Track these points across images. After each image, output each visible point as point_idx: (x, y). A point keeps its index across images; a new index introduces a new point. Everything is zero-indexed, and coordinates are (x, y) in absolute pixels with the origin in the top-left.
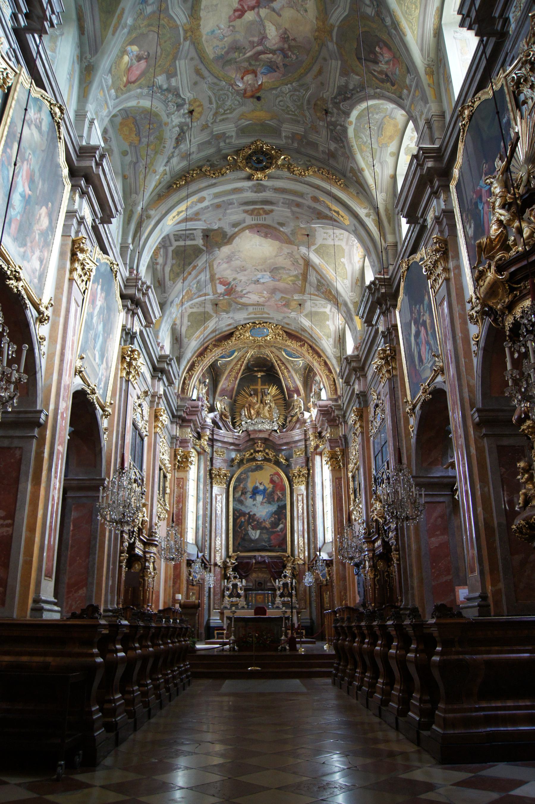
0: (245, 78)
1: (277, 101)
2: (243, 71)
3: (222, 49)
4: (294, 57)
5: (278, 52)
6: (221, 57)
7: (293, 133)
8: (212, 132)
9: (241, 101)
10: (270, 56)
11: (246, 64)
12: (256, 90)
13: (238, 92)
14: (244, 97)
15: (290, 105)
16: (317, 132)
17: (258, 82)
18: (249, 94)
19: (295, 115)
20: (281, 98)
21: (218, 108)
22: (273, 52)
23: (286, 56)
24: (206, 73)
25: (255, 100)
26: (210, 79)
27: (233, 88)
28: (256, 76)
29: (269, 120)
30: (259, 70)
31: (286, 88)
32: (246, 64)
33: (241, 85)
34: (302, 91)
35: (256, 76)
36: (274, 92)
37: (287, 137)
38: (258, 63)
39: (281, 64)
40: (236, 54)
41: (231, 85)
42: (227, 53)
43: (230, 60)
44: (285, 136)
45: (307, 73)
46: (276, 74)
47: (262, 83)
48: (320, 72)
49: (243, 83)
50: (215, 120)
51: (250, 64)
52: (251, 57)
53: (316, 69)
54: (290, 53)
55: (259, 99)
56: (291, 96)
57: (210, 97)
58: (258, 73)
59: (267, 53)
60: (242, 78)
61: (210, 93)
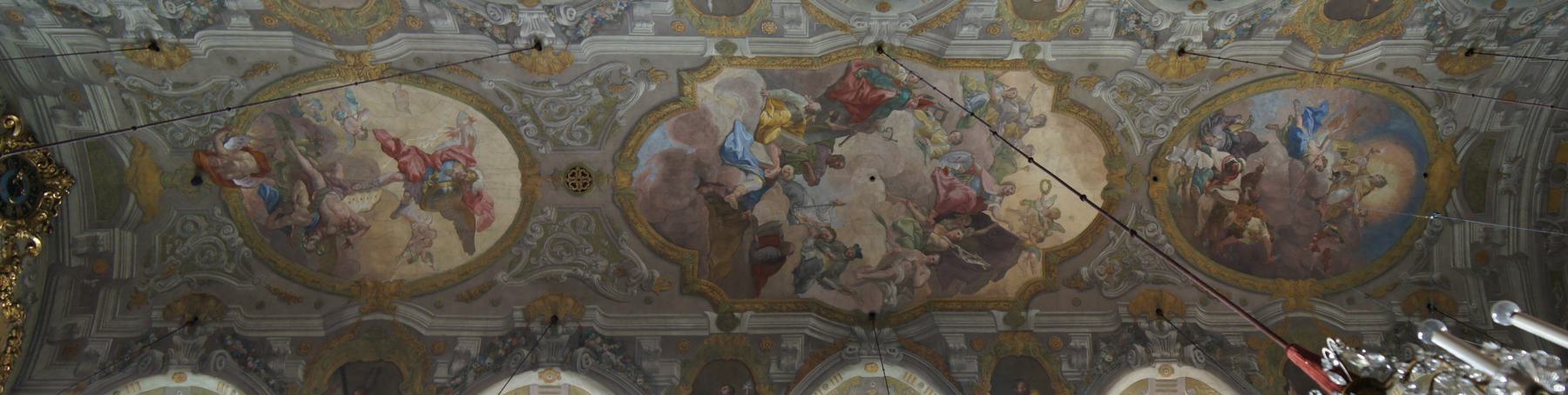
0: (246, 155)
1: (197, 218)
2: (265, 151)
3: (316, 115)
4: (311, 245)
5: (316, 216)
6: (296, 113)
7: (108, 257)
8: (90, 83)
9: (186, 145)
10: (306, 202)
11: (281, 155)
12: (219, 176)
13: (212, 139)
14: (196, 153)
15: (188, 243)
16: (128, 308)
17: (238, 178)
18: (206, 161)
19: (164, 256)
20: (202, 223)
21: (163, 98)
22: (315, 206)
23: (310, 230)
24: (257, 82)
25: (192, 174)
26: (241, 89)
27: (219, 131)
28: (253, 175)
29: (137, 201)
30: (270, 184)
31: (231, 233)
32: (281, 155)
33: (228, 146)
34: (233, 266)
35: (253, 175)
36: (218, 211)
37: (94, 241)
38: (285, 178)
39: (289, 223)
40: (304, 140)
41: (227, 127)
42: (306, 124)
43: (289, 129)
44: (96, 238)
45: (279, 274)
46: (263, 212)
47: (240, 187)
48: (287, 299)
49: (235, 151)
50: (127, 91)
51: (281, 165)
52: (300, 166)
53: (293, 289)
54: (317, 237)
55: (197, 181)
56: (214, 244)
57: (193, 85)
58: (261, 180)
59: (310, 195)
60: (246, 149)
61: (204, 86)
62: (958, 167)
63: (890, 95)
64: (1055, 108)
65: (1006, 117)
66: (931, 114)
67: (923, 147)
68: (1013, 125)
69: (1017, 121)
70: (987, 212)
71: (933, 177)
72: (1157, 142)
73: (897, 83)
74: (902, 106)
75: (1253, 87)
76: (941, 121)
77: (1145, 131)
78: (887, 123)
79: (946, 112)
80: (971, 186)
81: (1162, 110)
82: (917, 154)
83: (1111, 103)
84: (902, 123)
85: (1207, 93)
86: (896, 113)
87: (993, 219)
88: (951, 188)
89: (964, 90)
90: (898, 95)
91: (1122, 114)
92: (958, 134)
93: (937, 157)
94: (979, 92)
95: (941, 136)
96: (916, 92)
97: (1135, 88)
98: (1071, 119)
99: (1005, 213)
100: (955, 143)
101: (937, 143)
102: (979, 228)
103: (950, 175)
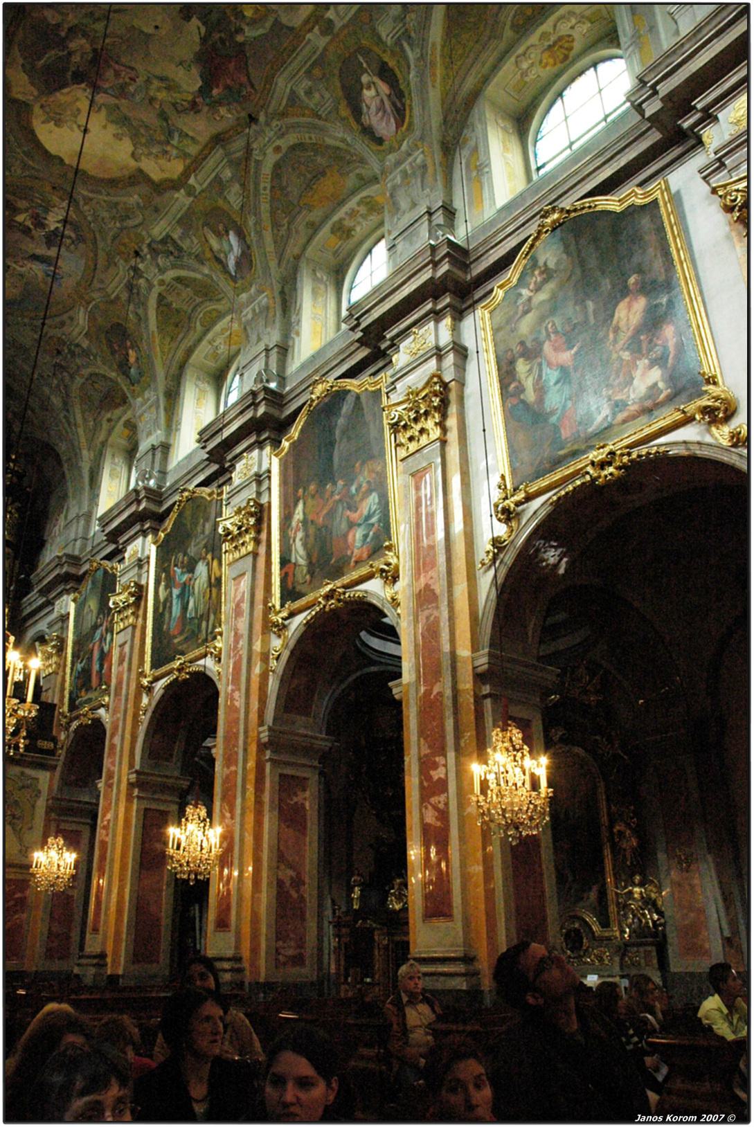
62: (132, 89)
63: (215, 92)
64: (140, 171)
65: (151, 141)
66: (184, 103)
67: (162, 79)
68: (143, 140)
69: (144, 145)
70: (83, 85)
71: (132, 69)
72: (81, 203)
73: (221, 104)
74: (201, 90)
75: (91, 264)
76: (174, 105)
77: (94, 202)
78: (195, 71)
79: (178, 112)
80: (111, 87)
81: (103, 219)
82: (158, 71)
83: (125, 199)
84: (190, 81)
85: (101, 245)
86: (200, 83)
87: (75, 86)
88: (117, 74)
89: (187, 135)
90: (212, 97)
91: (115, 199)
92: (158, 107)
93: (148, 81)
94: (180, 142)
95: (162, 95)
96: (206, 109)
97: (128, 217)
98: (126, 173)
99: (78, 96)
100: (152, 100)
101: (159, 89)
102: (74, 73)
103: (127, 80)
